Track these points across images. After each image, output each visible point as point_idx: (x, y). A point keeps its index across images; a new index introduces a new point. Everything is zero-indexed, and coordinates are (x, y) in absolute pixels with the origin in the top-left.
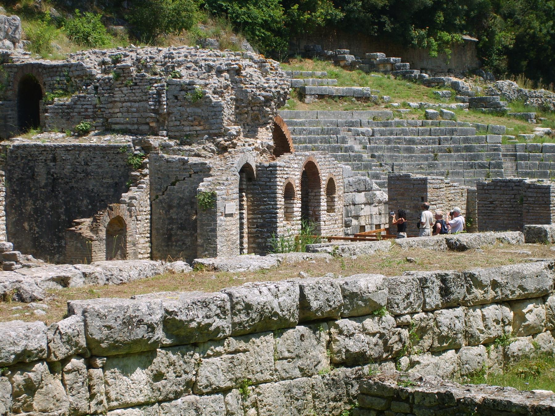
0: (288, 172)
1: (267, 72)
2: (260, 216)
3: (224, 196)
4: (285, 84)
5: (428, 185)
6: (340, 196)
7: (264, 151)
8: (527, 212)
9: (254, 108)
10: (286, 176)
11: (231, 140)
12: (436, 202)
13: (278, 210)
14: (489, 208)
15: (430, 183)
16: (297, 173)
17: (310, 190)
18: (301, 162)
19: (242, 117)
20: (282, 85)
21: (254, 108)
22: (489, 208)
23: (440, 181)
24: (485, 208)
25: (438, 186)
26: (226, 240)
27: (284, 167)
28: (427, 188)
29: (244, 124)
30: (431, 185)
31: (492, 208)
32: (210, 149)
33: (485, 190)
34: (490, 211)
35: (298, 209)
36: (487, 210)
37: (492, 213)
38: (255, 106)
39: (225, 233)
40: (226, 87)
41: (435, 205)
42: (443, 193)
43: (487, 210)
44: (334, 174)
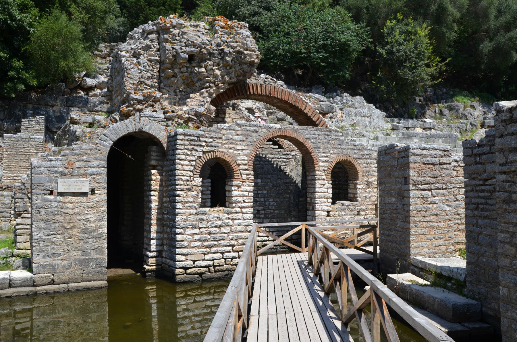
0: (213, 144)
1: (216, 32)
2: (168, 199)
3: (60, 170)
4: (237, 42)
5: (411, 159)
6: (368, 184)
7: (189, 120)
8: (505, 201)
9: (182, 70)
10: (206, 149)
11: (132, 106)
12: (433, 186)
13: (178, 193)
14: (482, 195)
15: (415, 155)
16: (239, 147)
17: (307, 173)
18: (255, 134)
19: (169, 81)
20: (230, 42)
21: (182, 70)
22: (482, 195)
23: (440, 153)
24: (476, 195)
25: (436, 160)
26: (64, 227)
27: (203, 136)
28: (408, 163)
29: (175, 92)
30: (418, 159)
31: (486, 194)
32: (114, 118)
33: (476, 155)
34: (483, 201)
35: (246, 193)
36: (479, 197)
37: (487, 204)
38: (183, 67)
39: (58, 218)
40: (147, 48)
41: (430, 190)
42: (447, 172)
43: (479, 197)
44: (355, 156)
